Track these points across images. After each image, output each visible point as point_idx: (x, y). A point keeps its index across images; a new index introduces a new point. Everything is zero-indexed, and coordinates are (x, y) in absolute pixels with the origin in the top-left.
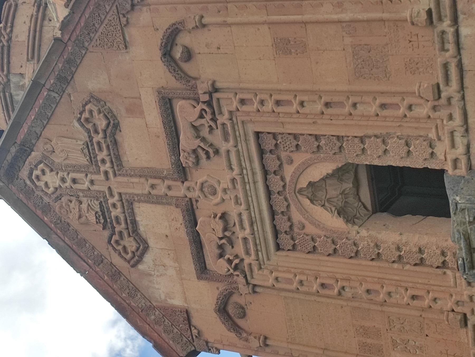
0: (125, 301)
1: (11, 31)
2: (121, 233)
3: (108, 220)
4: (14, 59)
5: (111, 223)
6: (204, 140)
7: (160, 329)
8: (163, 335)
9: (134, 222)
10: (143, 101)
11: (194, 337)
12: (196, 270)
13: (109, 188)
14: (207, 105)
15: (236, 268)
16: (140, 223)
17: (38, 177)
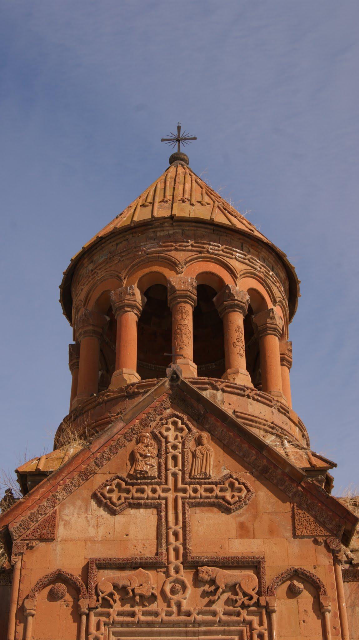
0: (62, 480)
1: (254, 399)
2: (128, 491)
3: (139, 481)
4: (234, 397)
5: (137, 484)
6: (223, 592)
7: (35, 510)
8: (29, 512)
9: (138, 506)
10: (252, 540)
11: (28, 542)
12: (99, 559)
13: (169, 490)
14: (255, 603)
15: (103, 599)
16: (138, 510)
17: (175, 423)
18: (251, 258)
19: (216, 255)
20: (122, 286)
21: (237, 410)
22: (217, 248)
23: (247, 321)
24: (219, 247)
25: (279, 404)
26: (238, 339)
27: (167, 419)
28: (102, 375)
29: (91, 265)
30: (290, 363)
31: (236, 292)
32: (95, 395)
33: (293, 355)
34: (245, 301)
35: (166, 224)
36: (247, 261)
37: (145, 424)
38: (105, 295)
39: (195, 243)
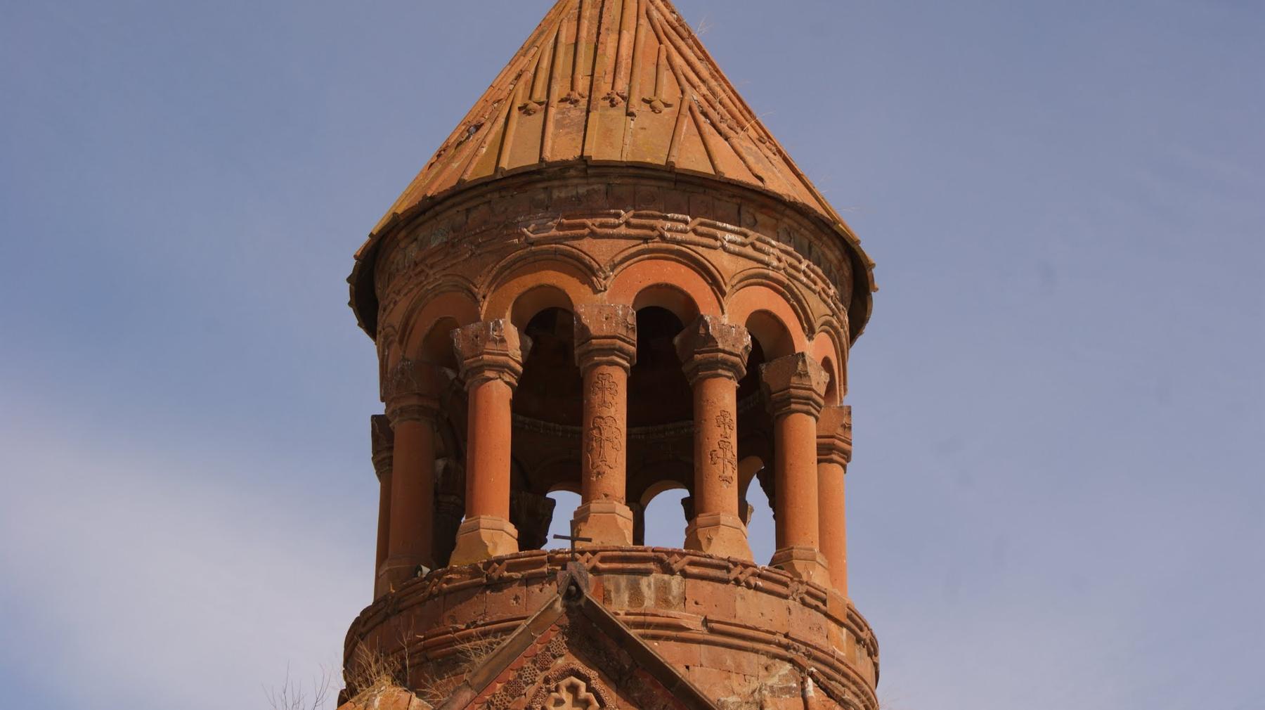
1: (749, 586)
4: (707, 587)
17: (573, 689)
18: (758, 239)
19: (679, 243)
20: (479, 320)
21: (710, 617)
22: (681, 226)
23: (749, 390)
24: (686, 223)
25: (803, 588)
26: (723, 444)
27: (557, 679)
28: (446, 468)
29: (414, 245)
30: (847, 455)
31: (721, 330)
32: (426, 570)
33: (855, 436)
34: (739, 349)
35: (572, 172)
36: (749, 250)
37: (514, 690)
38: (444, 328)
39: (634, 216)
